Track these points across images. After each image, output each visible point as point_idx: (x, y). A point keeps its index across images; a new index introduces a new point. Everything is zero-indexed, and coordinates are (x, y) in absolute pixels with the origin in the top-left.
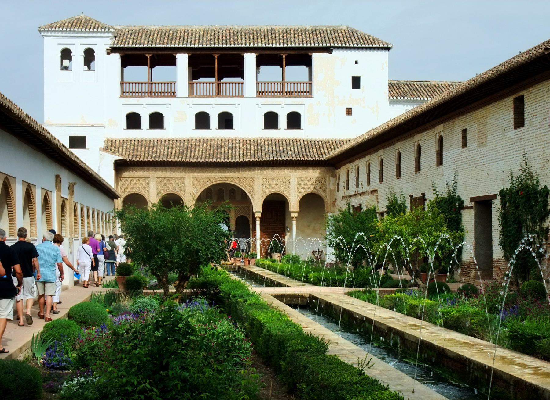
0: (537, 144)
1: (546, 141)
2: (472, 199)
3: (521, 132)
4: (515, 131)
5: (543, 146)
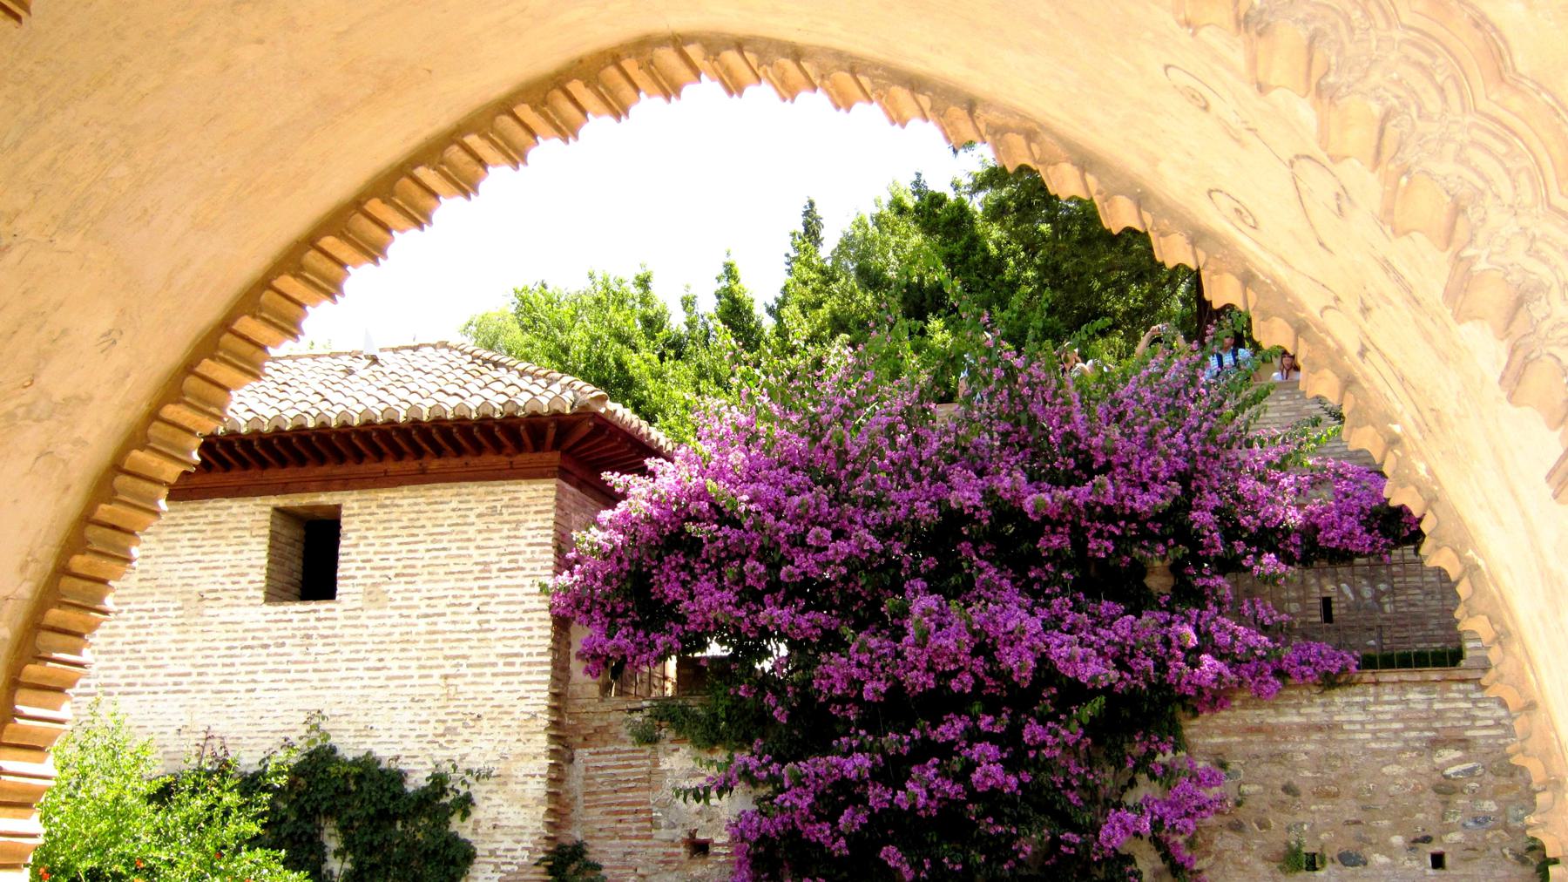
0: (415, 664)
1: (464, 657)
3: (312, 616)
4: (271, 609)
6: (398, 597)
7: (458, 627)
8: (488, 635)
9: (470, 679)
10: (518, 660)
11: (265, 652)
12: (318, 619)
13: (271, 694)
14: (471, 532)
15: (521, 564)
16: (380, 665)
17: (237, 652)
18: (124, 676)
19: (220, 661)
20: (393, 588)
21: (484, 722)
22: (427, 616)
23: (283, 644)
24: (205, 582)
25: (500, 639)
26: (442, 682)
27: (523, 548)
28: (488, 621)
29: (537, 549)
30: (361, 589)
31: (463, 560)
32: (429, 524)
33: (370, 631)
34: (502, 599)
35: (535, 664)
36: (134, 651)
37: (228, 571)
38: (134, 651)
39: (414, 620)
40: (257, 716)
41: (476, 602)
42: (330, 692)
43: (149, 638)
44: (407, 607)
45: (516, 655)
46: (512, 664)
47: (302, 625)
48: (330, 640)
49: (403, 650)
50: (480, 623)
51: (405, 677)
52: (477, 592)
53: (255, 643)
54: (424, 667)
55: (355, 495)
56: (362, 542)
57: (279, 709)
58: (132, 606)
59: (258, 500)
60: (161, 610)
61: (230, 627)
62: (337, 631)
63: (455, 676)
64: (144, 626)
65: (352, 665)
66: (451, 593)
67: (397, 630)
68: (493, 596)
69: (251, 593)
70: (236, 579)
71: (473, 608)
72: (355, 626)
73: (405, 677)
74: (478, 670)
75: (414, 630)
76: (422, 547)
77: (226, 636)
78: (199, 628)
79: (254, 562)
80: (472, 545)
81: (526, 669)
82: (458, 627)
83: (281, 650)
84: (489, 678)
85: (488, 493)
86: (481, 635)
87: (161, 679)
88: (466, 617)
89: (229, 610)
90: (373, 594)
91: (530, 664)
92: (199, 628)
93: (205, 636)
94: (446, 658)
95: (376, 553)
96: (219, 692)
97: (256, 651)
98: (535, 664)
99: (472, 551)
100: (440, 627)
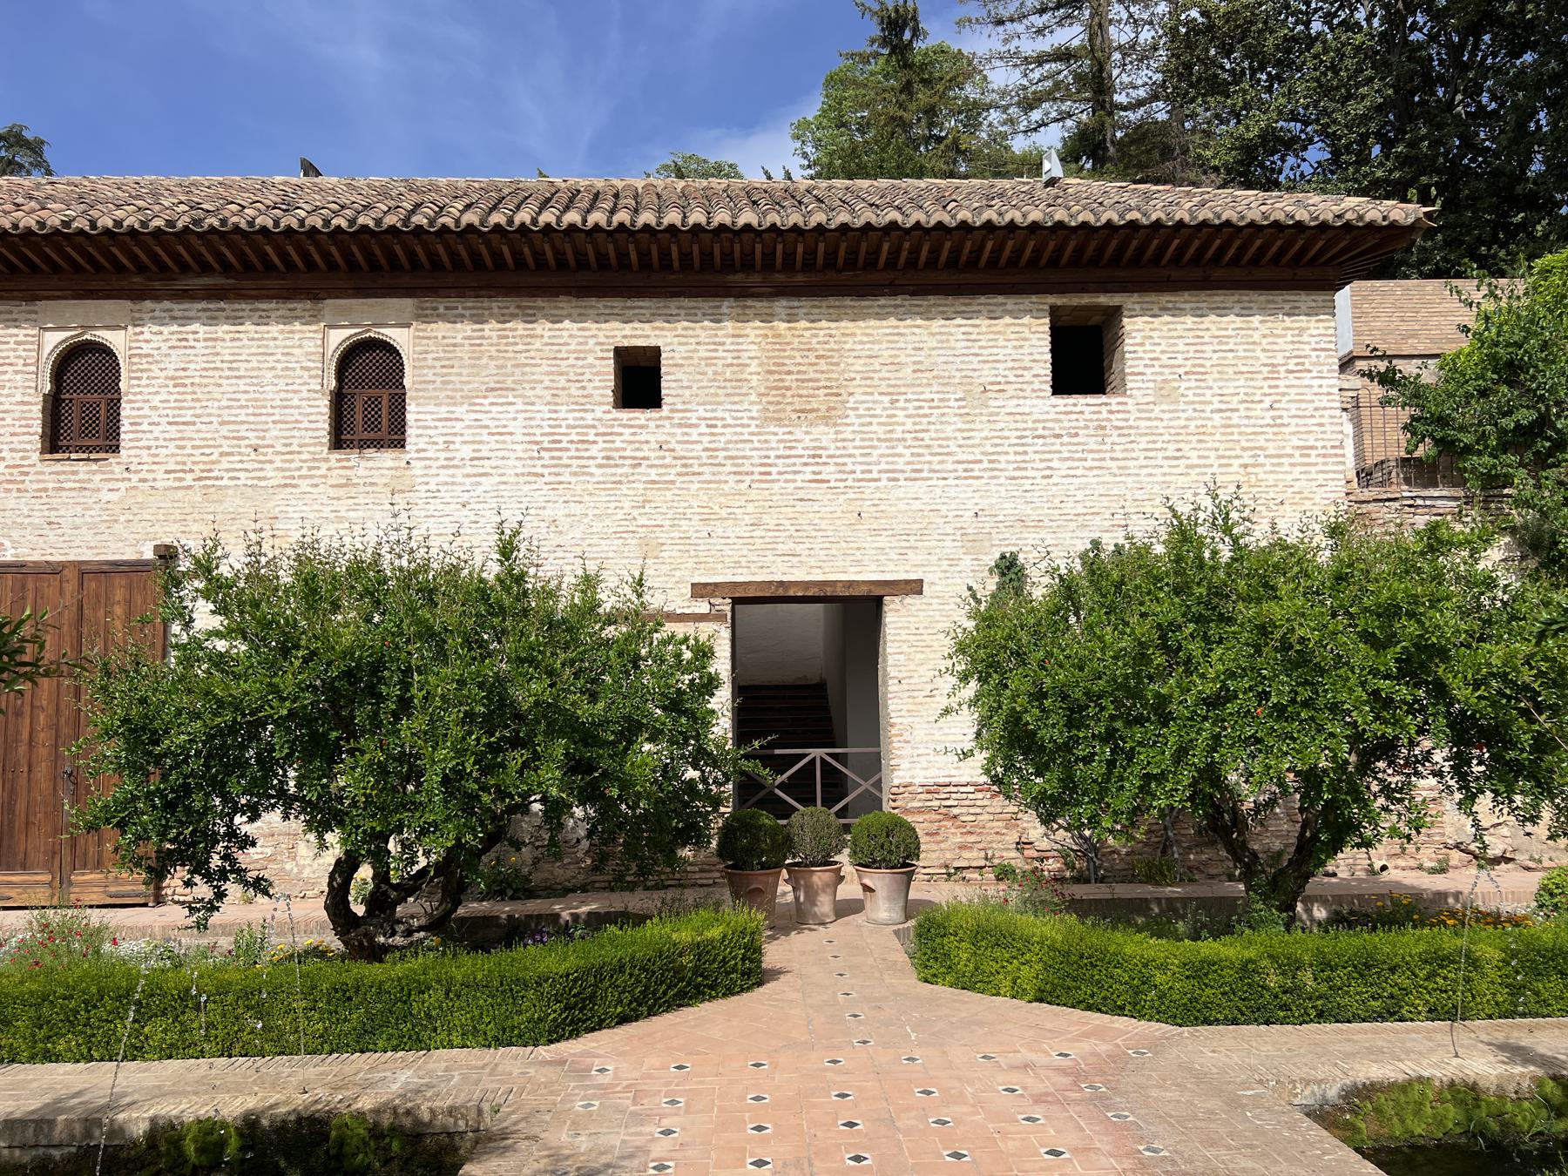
0: (1212, 454)
1: (1261, 448)
2: (700, 590)
3: (1104, 409)
5: (1246, 461)
6: (1190, 393)
7: (1253, 421)
8: (1283, 429)
9: (1268, 468)
10: (1314, 452)
11: (1058, 441)
12: (1111, 412)
13: (1070, 480)
14: (1256, 336)
15: (1307, 366)
16: (1178, 454)
17: (1029, 440)
18: (909, 463)
19: (1011, 450)
20: (1184, 385)
21: (1287, 507)
22: (1221, 411)
23: (1077, 435)
24: (987, 375)
25: (1294, 433)
26: (1242, 470)
27: (1308, 353)
28: (1281, 417)
29: (1323, 354)
30: (1151, 385)
31: (1250, 362)
32: (1213, 327)
33: (1165, 423)
34: (1292, 397)
35: (1330, 456)
36: (916, 439)
37: (1010, 364)
38: (916, 439)
39: (1208, 414)
40: (1057, 501)
41: (1268, 401)
42: (1130, 479)
43: (932, 427)
44: (1200, 403)
45: (1311, 448)
46: (1308, 456)
47: (1095, 417)
48: (1125, 432)
49: (1200, 441)
50: (1273, 418)
51: (1205, 466)
52: (1267, 391)
53: (1047, 433)
54: (1222, 457)
55: (1136, 297)
56: (1147, 342)
57: (1080, 495)
58: (909, 396)
59: (1034, 298)
60: (941, 400)
61: (1018, 417)
62: (1131, 423)
63: (1254, 466)
64: (925, 416)
65: (1151, 454)
66: (1242, 390)
67: (1193, 424)
68: (1284, 394)
69: (1037, 386)
70: (1020, 372)
71: (1266, 405)
72: (1149, 419)
73: (1205, 466)
74: (1275, 461)
75: (1210, 423)
76: (1209, 348)
77: (1013, 426)
78: (985, 419)
79: (1037, 357)
80: (1258, 348)
81: (1321, 460)
82: (1253, 421)
83: (1075, 440)
84: (1287, 468)
85: (1269, 302)
86: (1275, 429)
87: (950, 467)
88: (1258, 413)
89: (1015, 402)
90: (1165, 392)
91: (1325, 456)
92: (985, 419)
93: (993, 426)
94: (1244, 449)
95: (1163, 352)
96: (1013, 478)
97: (1048, 440)
98: (1330, 456)
99: (1259, 353)
100: (1235, 421)
